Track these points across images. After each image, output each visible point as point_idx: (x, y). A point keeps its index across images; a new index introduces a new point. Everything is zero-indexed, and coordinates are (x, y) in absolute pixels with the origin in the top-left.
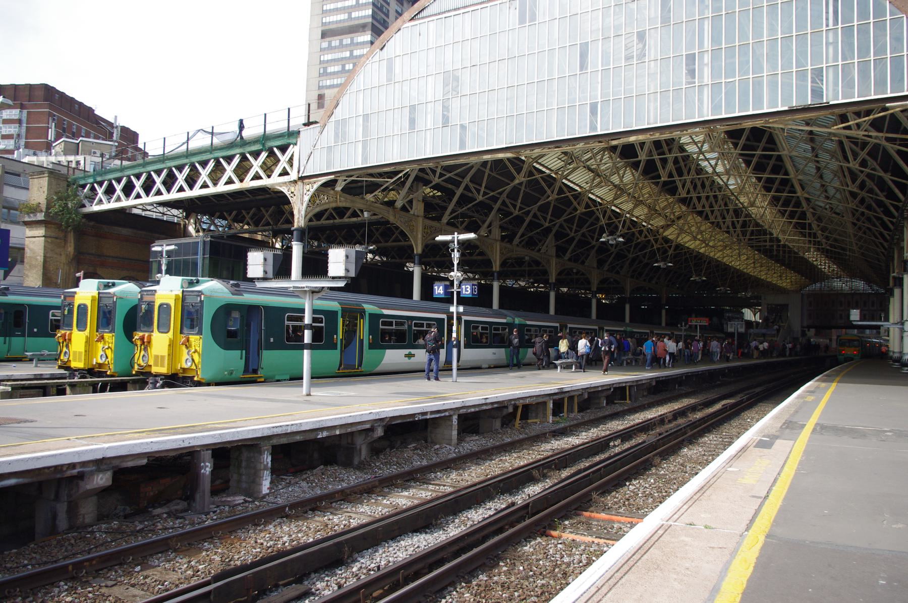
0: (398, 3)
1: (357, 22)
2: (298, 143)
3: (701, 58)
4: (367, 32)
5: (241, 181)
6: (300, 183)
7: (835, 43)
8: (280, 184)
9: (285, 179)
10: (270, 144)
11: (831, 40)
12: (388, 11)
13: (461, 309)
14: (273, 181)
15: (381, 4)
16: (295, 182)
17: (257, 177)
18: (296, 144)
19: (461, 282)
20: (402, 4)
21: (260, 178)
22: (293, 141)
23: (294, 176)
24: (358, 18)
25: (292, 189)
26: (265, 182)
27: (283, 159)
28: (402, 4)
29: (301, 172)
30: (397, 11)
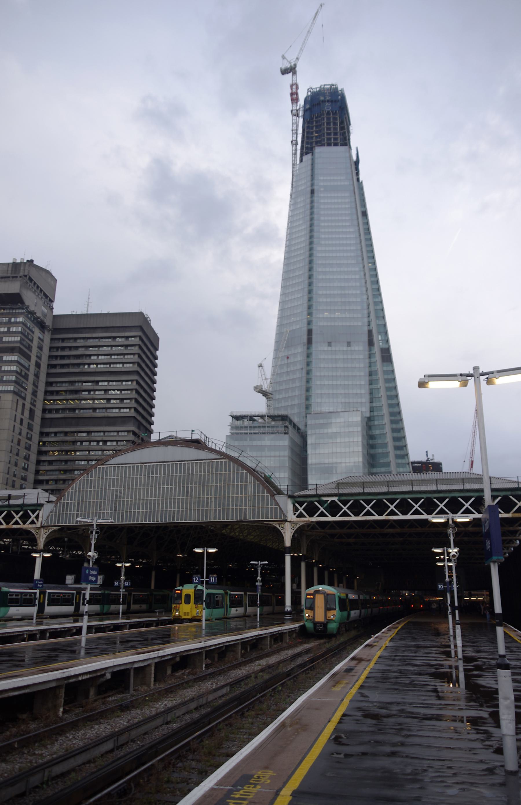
0: (41, 332)
1: (6, 345)
2: (42, 510)
3: (211, 499)
4: (15, 354)
5: (7, 524)
6: (42, 529)
7: (251, 500)
8: (30, 528)
9: (34, 526)
10: (25, 508)
11: (250, 499)
12: (33, 337)
13: (124, 590)
14: (27, 526)
15: (28, 333)
16: (39, 528)
17: (17, 523)
18: (41, 510)
19: (125, 580)
20: (44, 333)
21: (19, 524)
22: (39, 508)
23: (38, 525)
24: (9, 342)
25: (37, 531)
26: (21, 526)
27: (33, 516)
28: (44, 333)
29: (43, 524)
30: (39, 338)
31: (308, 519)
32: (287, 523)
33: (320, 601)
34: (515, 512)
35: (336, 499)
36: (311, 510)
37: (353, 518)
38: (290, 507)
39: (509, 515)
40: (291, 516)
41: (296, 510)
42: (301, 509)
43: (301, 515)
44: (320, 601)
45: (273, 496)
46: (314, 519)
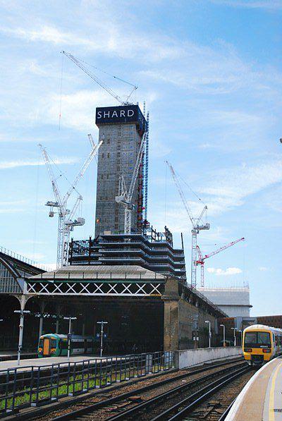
31: (35, 293)
32: (23, 296)
33: (47, 343)
34: (153, 293)
35: (52, 282)
36: (38, 288)
37: (62, 294)
38: (26, 285)
39: (149, 295)
40: (26, 292)
41: (29, 287)
42: (32, 287)
43: (32, 291)
44: (47, 343)
45: (15, 279)
46: (39, 294)
